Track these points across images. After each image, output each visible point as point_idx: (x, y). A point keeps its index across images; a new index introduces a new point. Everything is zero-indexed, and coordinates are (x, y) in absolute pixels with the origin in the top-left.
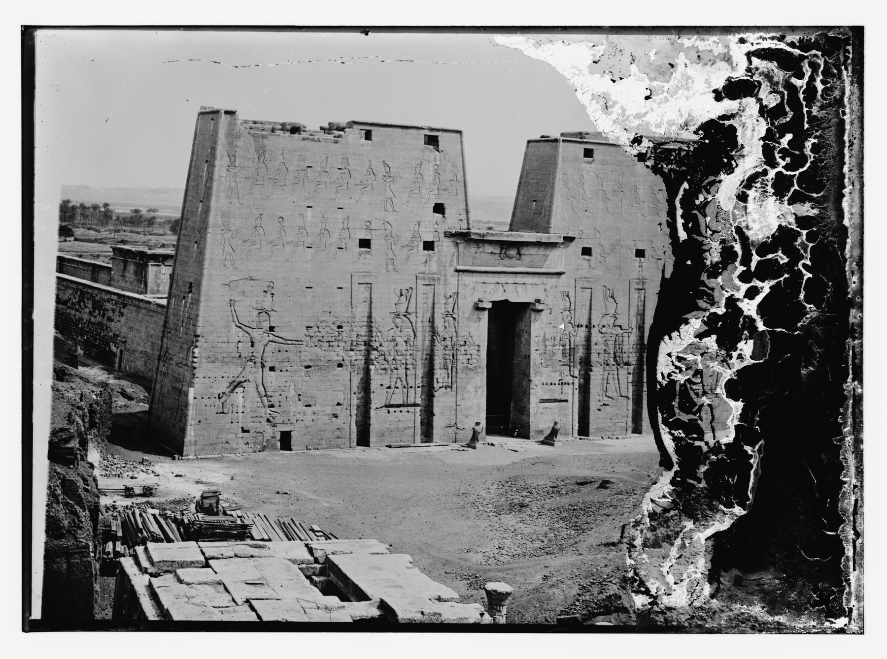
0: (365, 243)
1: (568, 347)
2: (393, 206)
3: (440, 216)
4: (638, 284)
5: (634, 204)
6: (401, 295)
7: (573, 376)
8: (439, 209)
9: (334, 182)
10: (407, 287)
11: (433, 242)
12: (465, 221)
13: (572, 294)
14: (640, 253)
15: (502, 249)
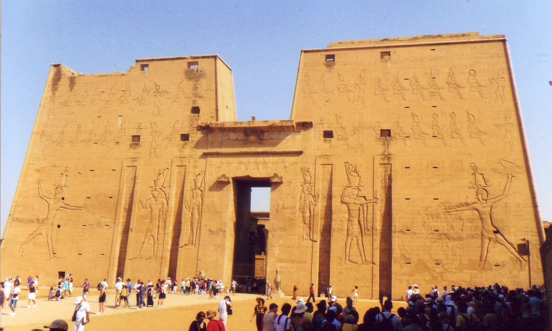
0: (136, 139)
1: (308, 214)
2: (159, 111)
3: (196, 115)
4: (383, 159)
5: (378, 92)
6: (160, 174)
7: (313, 241)
8: (196, 110)
9: (118, 100)
10: (165, 167)
11: (188, 135)
12: (215, 118)
13: (312, 170)
14: (386, 133)
15: (244, 135)
